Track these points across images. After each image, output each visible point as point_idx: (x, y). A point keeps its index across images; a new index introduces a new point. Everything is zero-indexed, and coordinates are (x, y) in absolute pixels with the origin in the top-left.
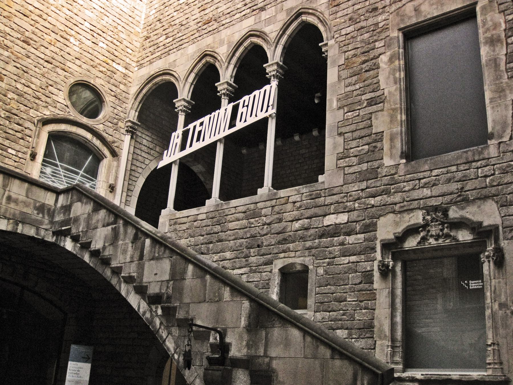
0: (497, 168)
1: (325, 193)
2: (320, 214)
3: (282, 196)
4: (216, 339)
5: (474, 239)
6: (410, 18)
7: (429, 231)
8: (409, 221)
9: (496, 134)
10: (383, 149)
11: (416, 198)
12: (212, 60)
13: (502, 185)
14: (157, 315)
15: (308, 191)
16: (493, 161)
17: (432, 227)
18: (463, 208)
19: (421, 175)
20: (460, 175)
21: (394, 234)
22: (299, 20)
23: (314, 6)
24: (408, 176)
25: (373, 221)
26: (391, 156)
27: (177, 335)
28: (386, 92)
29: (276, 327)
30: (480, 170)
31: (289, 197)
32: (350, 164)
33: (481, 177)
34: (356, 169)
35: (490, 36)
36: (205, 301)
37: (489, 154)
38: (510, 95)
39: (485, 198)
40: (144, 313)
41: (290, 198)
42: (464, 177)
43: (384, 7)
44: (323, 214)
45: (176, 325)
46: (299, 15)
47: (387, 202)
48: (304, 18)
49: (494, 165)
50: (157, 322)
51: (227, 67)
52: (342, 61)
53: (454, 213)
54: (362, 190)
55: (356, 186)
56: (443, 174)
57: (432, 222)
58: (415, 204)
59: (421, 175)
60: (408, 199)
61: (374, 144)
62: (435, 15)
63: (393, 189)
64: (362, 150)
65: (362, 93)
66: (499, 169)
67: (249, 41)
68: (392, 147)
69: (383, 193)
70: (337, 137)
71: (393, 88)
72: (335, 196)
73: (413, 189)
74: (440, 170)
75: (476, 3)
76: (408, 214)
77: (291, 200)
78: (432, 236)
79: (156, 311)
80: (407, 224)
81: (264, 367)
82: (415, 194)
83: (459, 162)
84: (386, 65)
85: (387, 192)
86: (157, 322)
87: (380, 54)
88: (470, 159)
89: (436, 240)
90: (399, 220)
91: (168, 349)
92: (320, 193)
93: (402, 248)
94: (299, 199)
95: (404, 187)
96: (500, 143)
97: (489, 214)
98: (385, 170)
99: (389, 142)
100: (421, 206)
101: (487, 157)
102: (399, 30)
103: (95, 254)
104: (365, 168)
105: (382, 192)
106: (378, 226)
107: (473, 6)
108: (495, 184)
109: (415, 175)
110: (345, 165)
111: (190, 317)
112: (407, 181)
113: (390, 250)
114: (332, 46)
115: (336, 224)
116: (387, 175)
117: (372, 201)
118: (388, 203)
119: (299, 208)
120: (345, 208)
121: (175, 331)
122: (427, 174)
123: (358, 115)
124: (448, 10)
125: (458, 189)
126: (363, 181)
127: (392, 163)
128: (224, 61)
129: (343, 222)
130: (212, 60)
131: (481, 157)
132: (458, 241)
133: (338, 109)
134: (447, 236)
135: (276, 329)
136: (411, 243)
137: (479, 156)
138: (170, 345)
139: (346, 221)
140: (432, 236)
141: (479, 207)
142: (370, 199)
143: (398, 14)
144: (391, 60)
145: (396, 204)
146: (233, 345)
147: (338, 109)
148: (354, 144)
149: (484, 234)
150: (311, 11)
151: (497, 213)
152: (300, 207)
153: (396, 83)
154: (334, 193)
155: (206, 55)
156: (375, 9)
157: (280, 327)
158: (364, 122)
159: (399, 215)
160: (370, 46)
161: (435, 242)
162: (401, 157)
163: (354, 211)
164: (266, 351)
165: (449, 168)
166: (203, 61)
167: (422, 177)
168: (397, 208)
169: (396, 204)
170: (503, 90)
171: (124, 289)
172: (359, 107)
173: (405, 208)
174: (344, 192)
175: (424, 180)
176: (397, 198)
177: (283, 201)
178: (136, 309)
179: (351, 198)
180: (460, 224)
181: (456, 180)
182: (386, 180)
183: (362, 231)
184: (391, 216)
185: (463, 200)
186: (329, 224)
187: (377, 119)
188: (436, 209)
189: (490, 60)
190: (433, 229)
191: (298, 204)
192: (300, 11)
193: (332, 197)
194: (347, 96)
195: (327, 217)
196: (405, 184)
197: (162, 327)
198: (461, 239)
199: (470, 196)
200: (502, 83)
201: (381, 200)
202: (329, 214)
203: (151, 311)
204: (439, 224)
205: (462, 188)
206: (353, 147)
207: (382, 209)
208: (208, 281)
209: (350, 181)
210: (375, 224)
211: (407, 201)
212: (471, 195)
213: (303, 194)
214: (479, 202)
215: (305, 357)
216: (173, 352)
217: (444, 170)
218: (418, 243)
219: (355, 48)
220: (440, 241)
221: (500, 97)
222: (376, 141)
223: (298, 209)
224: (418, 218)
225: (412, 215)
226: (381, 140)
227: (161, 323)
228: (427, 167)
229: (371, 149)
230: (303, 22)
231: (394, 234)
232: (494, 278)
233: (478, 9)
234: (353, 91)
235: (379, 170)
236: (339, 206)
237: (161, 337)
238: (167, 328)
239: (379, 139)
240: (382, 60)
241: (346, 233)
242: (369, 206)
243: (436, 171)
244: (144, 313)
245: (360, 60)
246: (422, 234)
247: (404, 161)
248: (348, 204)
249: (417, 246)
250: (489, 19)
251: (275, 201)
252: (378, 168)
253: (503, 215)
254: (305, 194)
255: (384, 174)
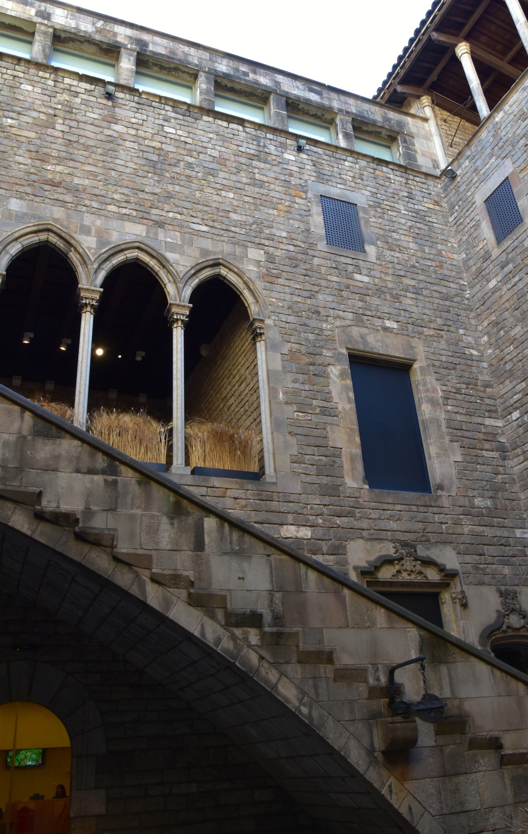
0: (450, 518)
1: (279, 497)
2: (274, 522)
3: (217, 486)
4: (378, 679)
5: (441, 580)
6: (357, 342)
7: (402, 565)
8: (380, 551)
9: (445, 487)
10: (342, 467)
11: (384, 528)
12: (62, 245)
13: (455, 534)
14: (250, 646)
15: (255, 488)
16: (446, 511)
17: (406, 562)
18: (428, 549)
19: (386, 506)
20: (421, 516)
21: (367, 562)
22: (216, 270)
23: (240, 266)
24: (374, 504)
25: (342, 543)
26: (354, 479)
27: (299, 676)
28: (340, 407)
29: (458, 662)
30: (436, 516)
31: (227, 489)
32: (308, 472)
33: (438, 523)
34: (314, 479)
35: (430, 396)
36: (348, 626)
37: (442, 503)
38: (452, 456)
39: (445, 543)
40: (218, 641)
41: (228, 490)
42: (424, 518)
43: (327, 316)
44: (279, 522)
45: (295, 659)
46: (216, 264)
47: (355, 525)
48: (223, 271)
49: (446, 514)
50: (254, 658)
51: (96, 271)
52: (285, 351)
53: (422, 552)
54: (325, 505)
55: (318, 500)
56: (405, 511)
57: (407, 557)
58: (383, 535)
59: (386, 506)
60: (376, 528)
61: (333, 459)
62: (381, 352)
63: (358, 513)
64: (319, 460)
65: (313, 397)
66: (452, 519)
67: (136, 254)
68: (353, 469)
69: (350, 515)
70: (287, 434)
71: (348, 407)
72: (292, 504)
73: (379, 519)
74: (403, 506)
75: (415, 360)
76: (379, 543)
77: (229, 493)
78: (406, 570)
79: (246, 639)
80: (379, 554)
81: (455, 711)
82: (383, 524)
83: (418, 503)
84: (337, 378)
85: (350, 514)
86: (254, 658)
87: (329, 364)
88: (428, 504)
89: (409, 575)
90: (370, 548)
91: (288, 700)
92: (272, 496)
93: (376, 578)
94: (243, 496)
95: (370, 514)
96: (449, 496)
97: (449, 558)
98: (349, 491)
99: (349, 461)
100: (389, 538)
101: (441, 506)
102: (347, 349)
103: (61, 520)
104: (325, 482)
105: (348, 514)
106: (348, 550)
107: (412, 362)
108: (451, 532)
109: (381, 505)
110: (301, 471)
111: (327, 649)
112: (372, 509)
113: (364, 578)
114: (269, 326)
115: (297, 538)
116: (352, 496)
117: (338, 521)
118: (355, 527)
119: (244, 508)
120: (306, 522)
121: (295, 670)
122: (391, 507)
123: (310, 420)
124: (393, 354)
125: (420, 529)
126: (325, 495)
127: (355, 485)
128: (93, 259)
129: (306, 537)
130: (62, 245)
131: (437, 504)
132: (428, 579)
133: (285, 403)
134: (420, 573)
135: (459, 664)
136: (386, 574)
137: (435, 502)
138: (288, 692)
139: (309, 537)
140: (406, 570)
141: (441, 550)
142: (336, 518)
143: (344, 331)
144: (342, 375)
145: (363, 530)
146: (406, 687)
147: (285, 403)
148: (309, 450)
149: (450, 576)
150: (236, 270)
151: (456, 559)
152: (246, 506)
153: (350, 402)
154: (291, 500)
155: (49, 230)
156: (318, 313)
157: (463, 662)
158: (319, 430)
159: (369, 543)
160: (318, 350)
161: (408, 577)
162: (365, 483)
163: (317, 526)
164: (452, 691)
165: (411, 507)
166: (43, 237)
167: (386, 508)
168: (365, 534)
169: (363, 530)
170: (446, 450)
171: (153, 596)
172: (312, 412)
173: (374, 537)
174: (303, 502)
175: (389, 512)
176: (365, 524)
177: (219, 492)
178: (197, 633)
179: (312, 511)
180: (428, 562)
181: (418, 520)
182: (351, 502)
183: (331, 553)
184: (360, 542)
185: (426, 541)
186: (289, 536)
187: (334, 433)
188: (405, 544)
189: (433, 419)
190: (408, 564)
191: (243, 502)
192: (221, 261)
193: (289, 504)
194: (296, 393)
195: (285, 527)
196: (371, 511)
197: (266, 665)
198: (430, 578)
199: (431, 538)
200: (444, 443)
201: (348, 522)
202: (287, 524)
203: (233, 637)
204: (413, 561)
205: (424, 529)
206: (309, 453)
207: (349, 531)
208: (347, 599)
209: (310, 492)
210: (345, 547)
211: (374, 530)
212: (433, 538)
213: (248, 490)
214: (441, 546)
215: (500, 696)
216: (297, 704)
217: (407, 507)
218: (393, 576)
219: (299, 344)
220: (413, 576)
221: (444, 455)
222: (334, 456)
223: (243, 508)
224: (389, 549)
225: (382, 545)
226: (339, 456)
227: (262, 658)
228: (390, 500)
229: (331, 463)
230: (219, 275)
231: (367, 562)
232: (462, 619)
233: (416, 366)
234: (302, 390)
235: (340, 488)
236: (299, 517)
237: (267, 681)
238: (275, 665)
239: (338, 455)
240: (331, 371)
241: (311, 551)
242: (335, 526)
243: (399, 506)
244: (218, 641)
245: (307, 360)
246: (397, 567)
247: (367, 487)
248: (311, 518)
249: (391, 578)
250: (428, 381)
251: (205, 488)
252: (339, 486)
253: (460, 562)
254: (250, 491)
255: (348, 495)
